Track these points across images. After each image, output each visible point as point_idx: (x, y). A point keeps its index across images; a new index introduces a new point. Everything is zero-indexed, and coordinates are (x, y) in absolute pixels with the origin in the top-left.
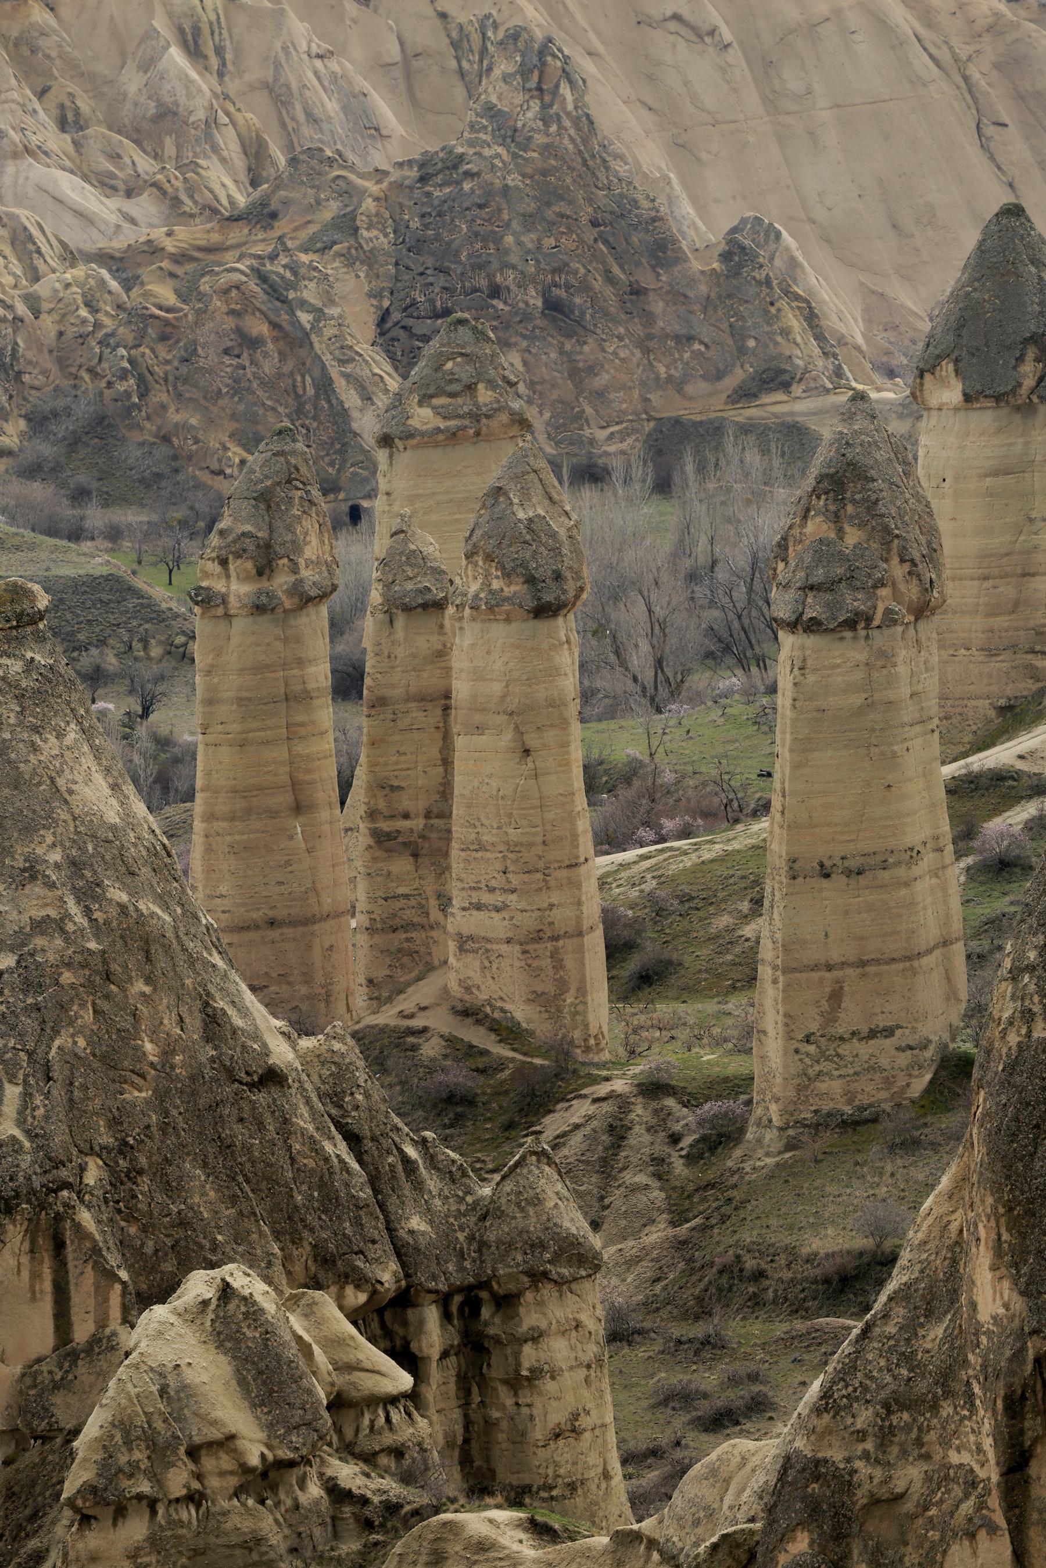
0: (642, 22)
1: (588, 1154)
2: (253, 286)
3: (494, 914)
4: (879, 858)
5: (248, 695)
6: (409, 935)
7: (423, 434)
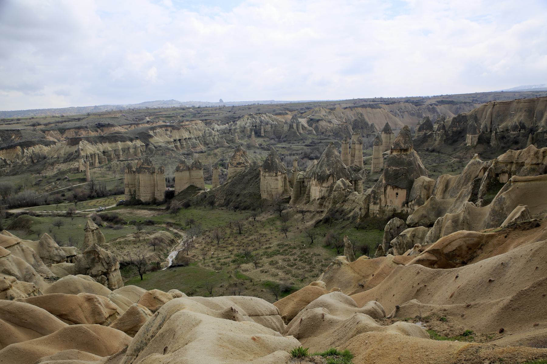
0: (367, 112)
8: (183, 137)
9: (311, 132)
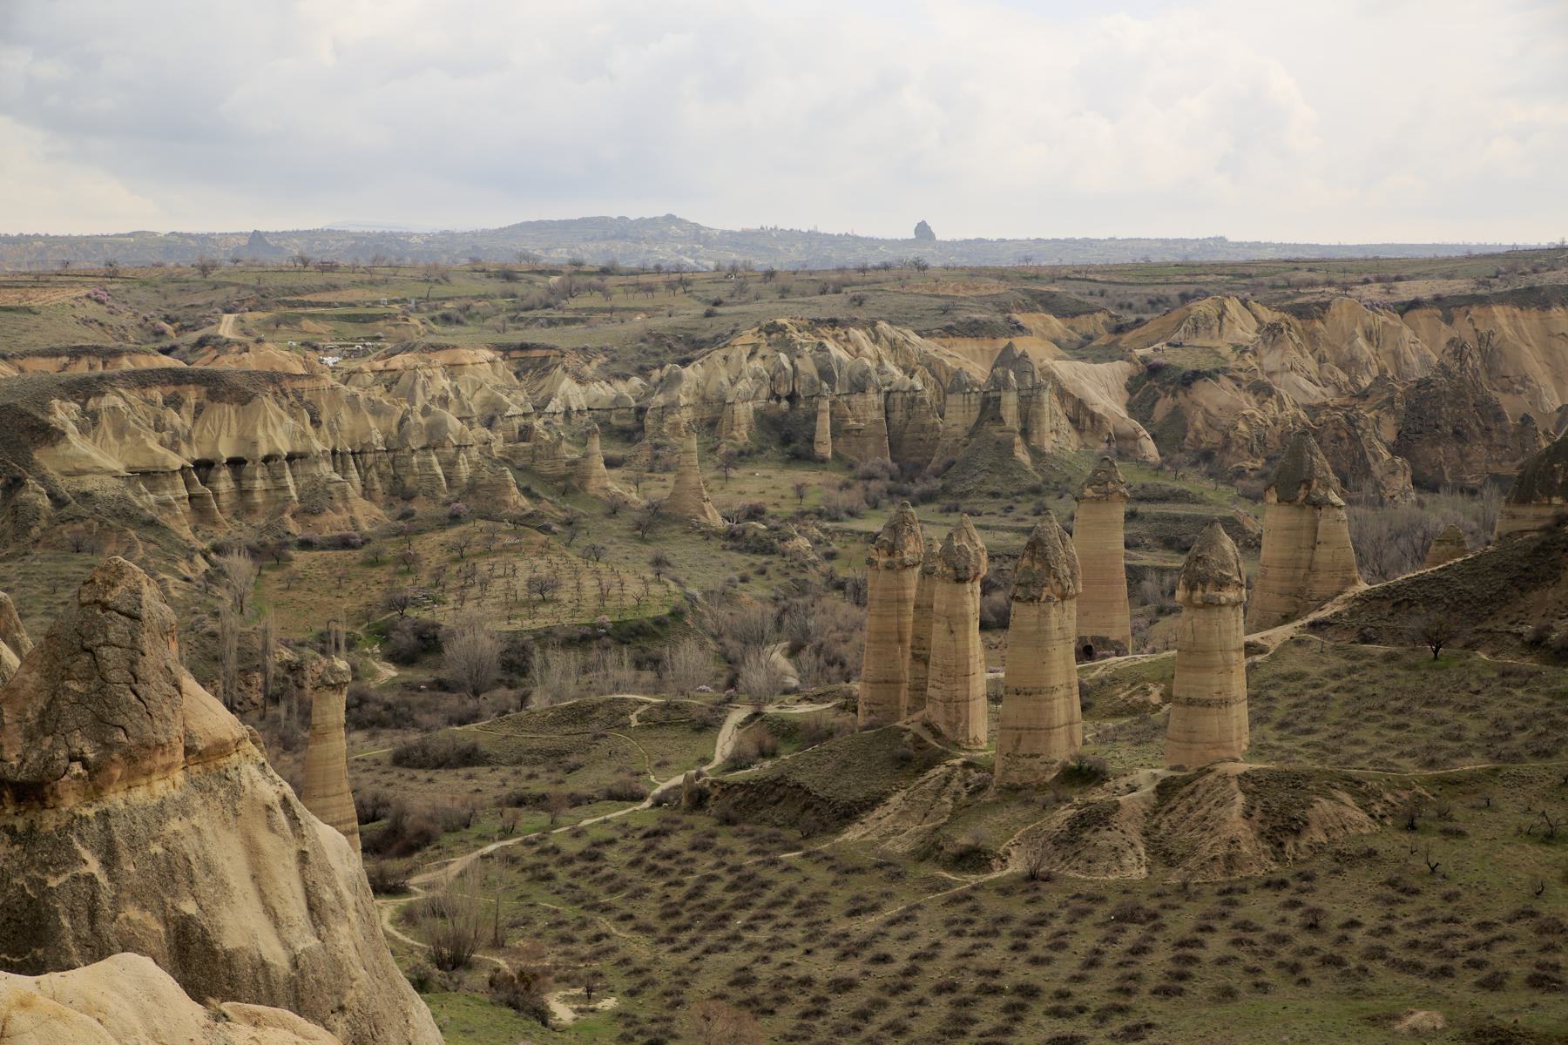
0: (1551, 335)
2: (1343, 420)
8: (255, 444)
9: (1130, 444)
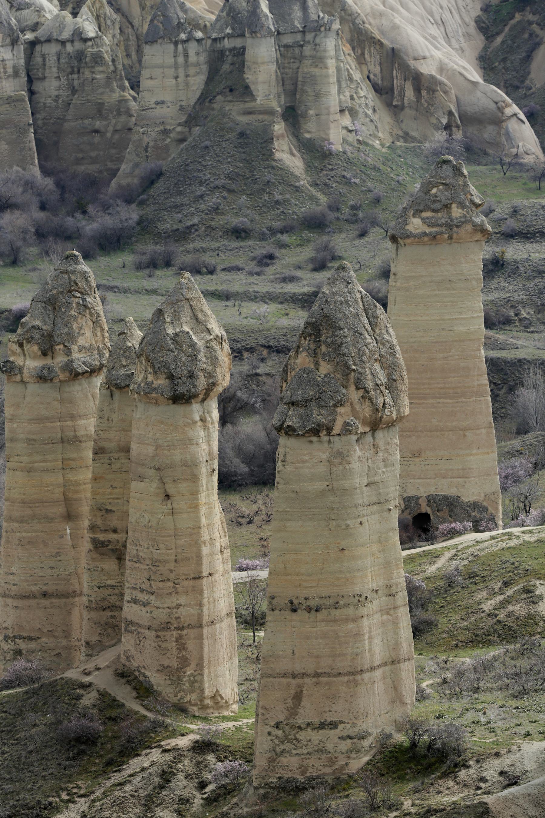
1: (140, 791)
3: (143, 608)
4: (332, 601)
5: (34, 437)
6: (113, 613)
7: (415, 236)
9: (489, 132)
